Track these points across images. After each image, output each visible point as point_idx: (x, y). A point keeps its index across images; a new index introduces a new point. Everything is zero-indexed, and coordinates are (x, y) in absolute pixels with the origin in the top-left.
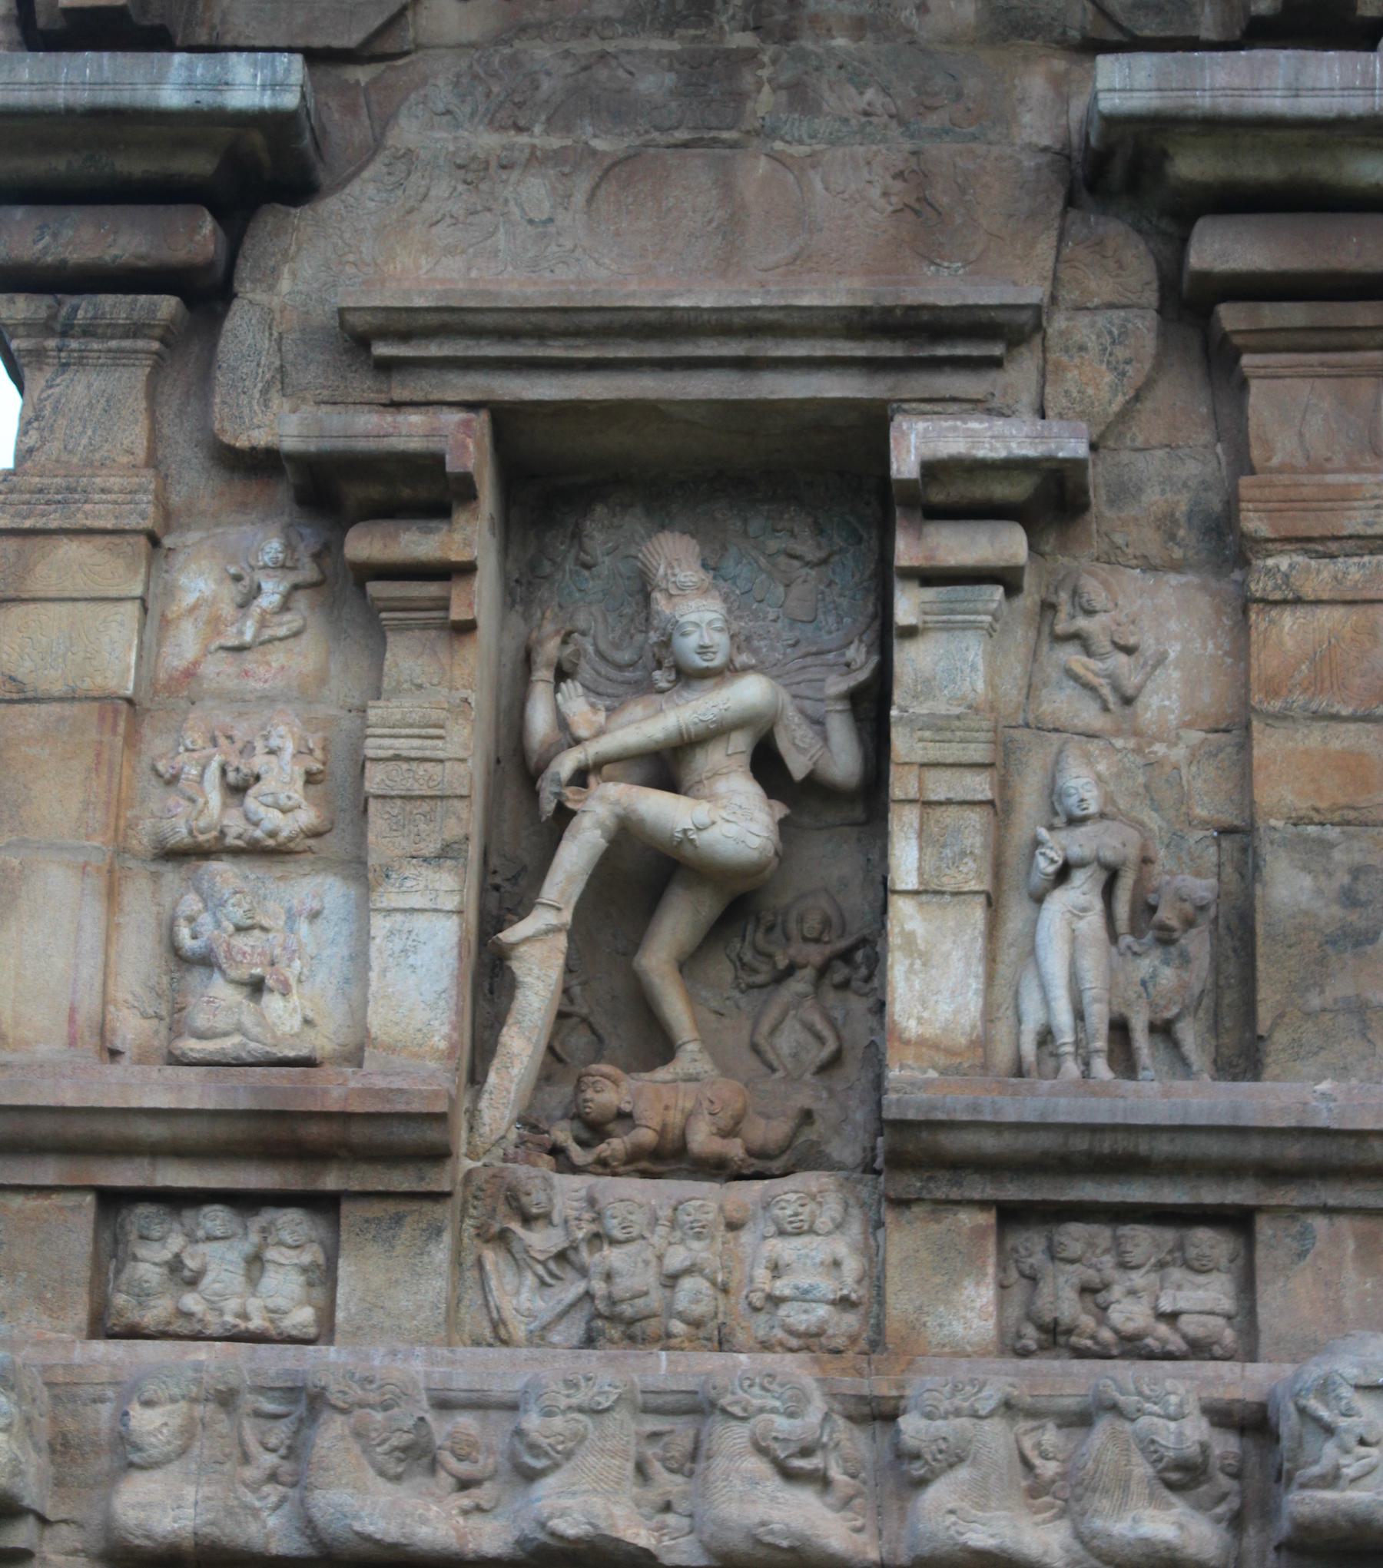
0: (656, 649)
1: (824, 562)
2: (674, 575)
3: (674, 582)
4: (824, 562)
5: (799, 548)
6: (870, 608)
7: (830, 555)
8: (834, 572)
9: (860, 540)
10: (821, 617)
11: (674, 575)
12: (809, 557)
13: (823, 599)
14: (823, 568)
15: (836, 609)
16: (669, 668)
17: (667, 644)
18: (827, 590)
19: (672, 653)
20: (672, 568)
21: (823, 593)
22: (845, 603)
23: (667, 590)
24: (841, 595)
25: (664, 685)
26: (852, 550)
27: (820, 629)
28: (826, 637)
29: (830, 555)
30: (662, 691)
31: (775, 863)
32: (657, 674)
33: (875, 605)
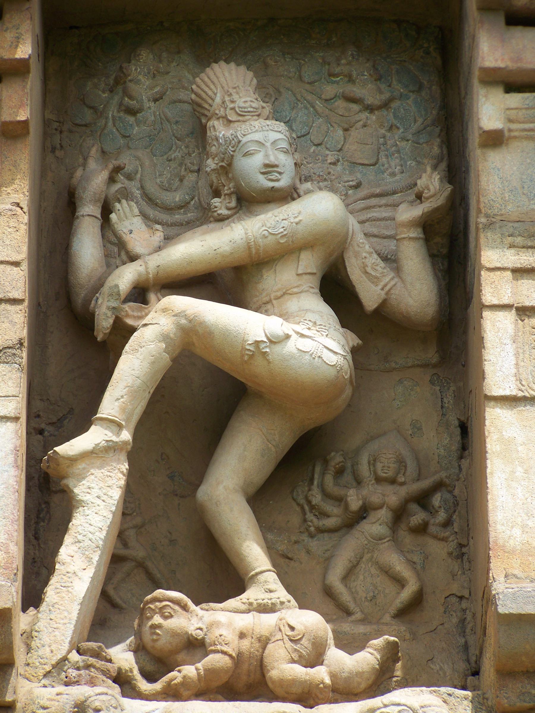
0: (214, 177)
1: (385, 105)
2: (233, 102)
3: (233, 109)
4: (385, 105)
5: (357, 91)
6: (436, 150)
7: (391, 100)
8: (395, 116)
9: (421, 87)
10: (383, 160)
11: (233, 102)
12: (370, 100)
13: (385, 144)
14: (384, 112)
15: (398, 152)
16: (229, 195)
17: (227, 168)
18: (388, 134)
19: (234, 179)
20: (230, 95)
21: (384, 137)
22: (406, 146)
23: (225, 117)
24: (403, 139)
25: (224, 212)
26: (413, 96)
27: (383, 172)
28: (389, 179)
29: (391, 100)
30: (221, 219)
31: (348, 391)
32: (216, 201)
33: (441, 147)
